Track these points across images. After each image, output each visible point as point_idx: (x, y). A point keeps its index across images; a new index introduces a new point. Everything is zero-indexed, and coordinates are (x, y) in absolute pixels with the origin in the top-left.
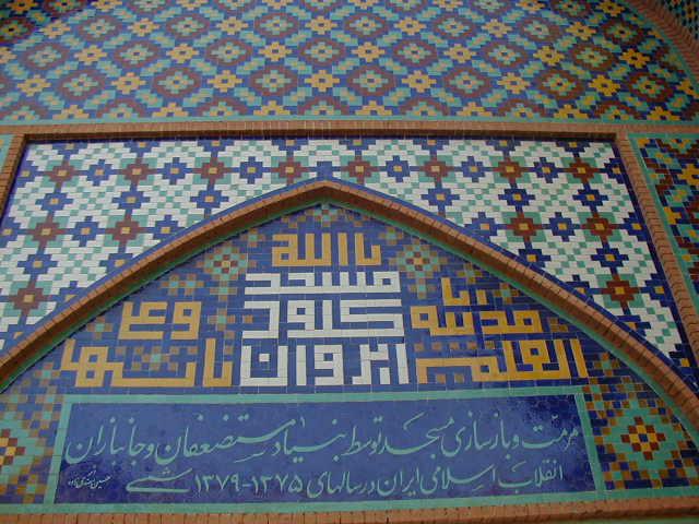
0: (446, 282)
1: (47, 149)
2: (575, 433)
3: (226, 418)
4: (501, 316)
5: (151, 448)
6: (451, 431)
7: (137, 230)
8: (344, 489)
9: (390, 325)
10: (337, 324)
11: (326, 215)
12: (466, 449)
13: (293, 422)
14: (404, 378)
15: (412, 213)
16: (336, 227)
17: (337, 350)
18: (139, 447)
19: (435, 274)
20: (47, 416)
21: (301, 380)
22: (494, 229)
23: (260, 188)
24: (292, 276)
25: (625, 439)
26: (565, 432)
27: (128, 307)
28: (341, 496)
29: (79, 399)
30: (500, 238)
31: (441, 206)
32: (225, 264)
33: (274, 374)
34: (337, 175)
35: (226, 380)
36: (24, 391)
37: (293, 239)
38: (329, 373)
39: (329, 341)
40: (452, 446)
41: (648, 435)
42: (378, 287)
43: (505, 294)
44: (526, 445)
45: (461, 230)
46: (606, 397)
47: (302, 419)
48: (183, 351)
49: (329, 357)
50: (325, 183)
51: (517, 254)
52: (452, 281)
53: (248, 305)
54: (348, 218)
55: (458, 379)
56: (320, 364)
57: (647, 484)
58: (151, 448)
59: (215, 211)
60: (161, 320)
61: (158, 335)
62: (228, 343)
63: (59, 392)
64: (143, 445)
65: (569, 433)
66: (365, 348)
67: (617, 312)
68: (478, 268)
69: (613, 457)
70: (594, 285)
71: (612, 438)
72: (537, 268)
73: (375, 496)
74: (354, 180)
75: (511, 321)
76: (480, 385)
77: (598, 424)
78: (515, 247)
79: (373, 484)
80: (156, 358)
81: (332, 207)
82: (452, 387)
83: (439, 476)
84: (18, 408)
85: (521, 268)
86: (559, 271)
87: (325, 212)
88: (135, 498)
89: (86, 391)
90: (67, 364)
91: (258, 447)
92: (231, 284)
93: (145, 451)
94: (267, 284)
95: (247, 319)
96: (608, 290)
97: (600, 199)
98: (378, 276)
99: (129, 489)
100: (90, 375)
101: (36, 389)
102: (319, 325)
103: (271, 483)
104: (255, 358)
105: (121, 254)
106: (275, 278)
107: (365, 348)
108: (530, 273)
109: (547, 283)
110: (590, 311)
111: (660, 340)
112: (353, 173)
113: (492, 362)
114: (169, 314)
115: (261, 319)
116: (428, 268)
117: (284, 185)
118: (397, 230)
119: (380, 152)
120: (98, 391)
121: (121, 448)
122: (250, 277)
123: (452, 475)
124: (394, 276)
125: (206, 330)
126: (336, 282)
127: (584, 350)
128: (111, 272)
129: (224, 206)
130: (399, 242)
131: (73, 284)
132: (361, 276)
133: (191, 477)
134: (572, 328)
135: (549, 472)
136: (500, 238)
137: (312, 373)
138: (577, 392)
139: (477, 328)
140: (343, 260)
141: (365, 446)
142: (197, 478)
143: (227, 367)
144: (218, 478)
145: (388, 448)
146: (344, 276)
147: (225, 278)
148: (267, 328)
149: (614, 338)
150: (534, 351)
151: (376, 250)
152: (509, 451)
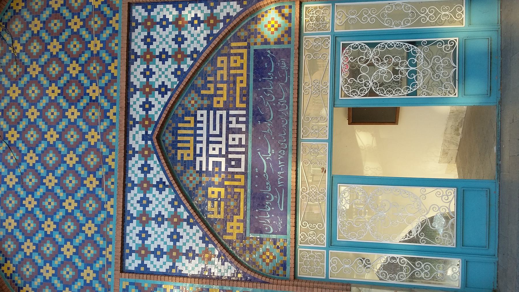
0: (203, 92)
1: (127, 262)
2: (269, 51)
3: (257, 177)
7: (175, 215)
9: (221, 116)
10: (220, 135)
11: (168, 138)
13: (259, 153)
14: (244, 112)
15: (171, 102)
16: (175, 134)
17: (231, 136)
21: (243, 149)
22: (179, 69)
26: (268, 55)
28: (287, 137)
30: (185, 67)
31: (167, 90)
32: (191, 178)
33: (239, 160)
34: (150, 132)
35: (242, 177)
37: (180, 152)
38: (240, 139)
39: (227, 139)
41: (271, 25)
43: (209, 69)
45: (181, 82)
49: (234, 139)
50: (154, 138)
53: (210, 169)
56: (237, 142)
58: (267, 203)
59: (167, 183)
60: (216, 203)
61: (222, 203)
64: (266, 206)
65: (269, 54)
66: (231, 126)
67: (221, 25)
68: (197, 78)
69: (279, 39)
74: (153, 125)
75: (222, 69)
76: (248, 84)
78: (189, 62)
79: (283, 126)
80: (232, 203)
81: (164, 135)
82: (247, 95)
83: (282, 103)
86: (202, 45)
87: (167, 138)
90: (234, 238)
91: (268, 165)
92: (201, 176)
95: (217, 169)
96: (212, 27)
97: (165, 18)
98: (199, 118)
100: (238, 228)
102: (220, 143)
103: (282, 160)
104: (233, 167)
105: (187, 221)
107: (231, 126)
109: (207, 51)
111: (235, 10)
112: (149, 125)
113: (239, 79)
114: (213, 200)
115: (217, 164)
116: (196, 98)
119: (137, 112)
121: (267, 213)
122: (198, 169)
124: (199, 112)
125: (221, 185)
126: (201, 135)
128: (196, 223)
129: (165, 179)
131: (200, 238)
132: (199, 125)
133: (278, 188)
135: (283, 64)
136: (185, 67)
137: (240, 145)
138: (253, 48)
140: (191, 132)
143: (236, 177)
144: (279, 179)
145: (270, 120)
146: (199, 132)
147: (198, 179)
149: (233, 29)
150: (235, 61)
151: (187, 119)
152: (274, 77)
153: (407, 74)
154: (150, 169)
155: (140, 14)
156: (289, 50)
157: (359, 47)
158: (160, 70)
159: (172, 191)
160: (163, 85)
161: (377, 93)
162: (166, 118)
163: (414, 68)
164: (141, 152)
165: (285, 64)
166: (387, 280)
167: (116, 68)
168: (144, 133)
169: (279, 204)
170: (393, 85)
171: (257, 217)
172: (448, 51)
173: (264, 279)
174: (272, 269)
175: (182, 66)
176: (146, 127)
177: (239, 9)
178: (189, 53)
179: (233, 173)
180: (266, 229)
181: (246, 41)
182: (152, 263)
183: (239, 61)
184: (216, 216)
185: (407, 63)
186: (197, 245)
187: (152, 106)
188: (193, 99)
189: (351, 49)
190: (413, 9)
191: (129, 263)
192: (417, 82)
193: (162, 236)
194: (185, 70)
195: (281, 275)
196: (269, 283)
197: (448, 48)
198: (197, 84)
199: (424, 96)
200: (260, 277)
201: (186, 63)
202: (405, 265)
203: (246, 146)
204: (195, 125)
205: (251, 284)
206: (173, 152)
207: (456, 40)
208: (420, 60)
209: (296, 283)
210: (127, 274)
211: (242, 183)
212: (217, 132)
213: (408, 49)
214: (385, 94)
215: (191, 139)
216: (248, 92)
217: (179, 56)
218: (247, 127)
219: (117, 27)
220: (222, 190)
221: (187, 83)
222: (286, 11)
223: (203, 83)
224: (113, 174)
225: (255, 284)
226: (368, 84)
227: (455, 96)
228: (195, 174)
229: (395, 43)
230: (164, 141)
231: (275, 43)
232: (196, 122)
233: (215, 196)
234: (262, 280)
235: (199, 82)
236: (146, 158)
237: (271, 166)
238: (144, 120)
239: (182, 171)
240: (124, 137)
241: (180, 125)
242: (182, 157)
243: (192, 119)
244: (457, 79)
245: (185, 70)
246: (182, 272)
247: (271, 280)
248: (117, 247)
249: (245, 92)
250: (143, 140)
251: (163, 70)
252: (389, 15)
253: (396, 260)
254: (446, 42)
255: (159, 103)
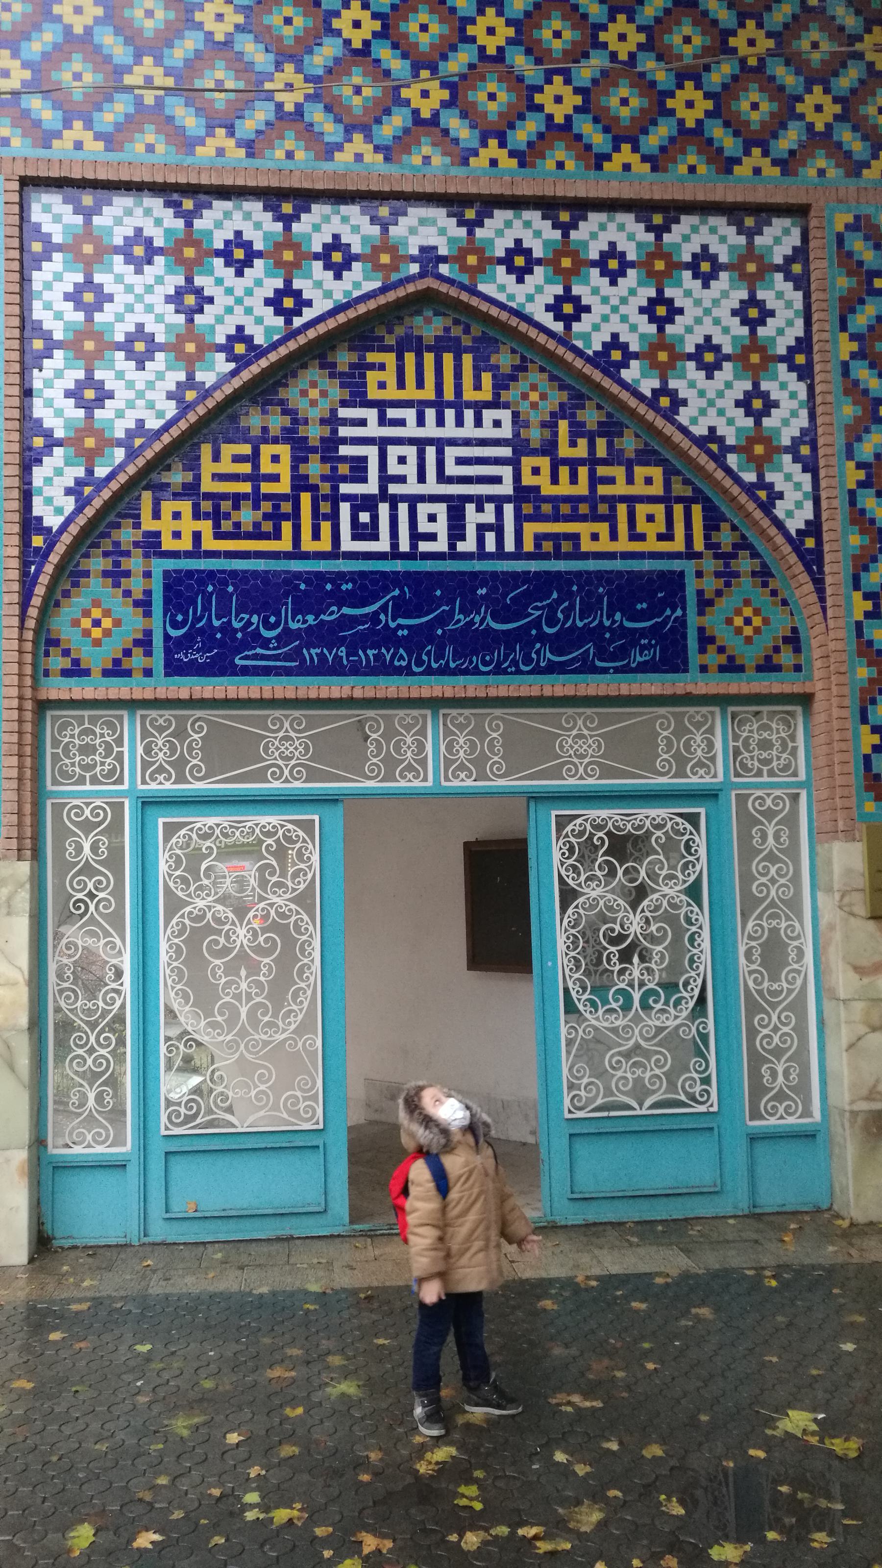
0: (563, 426)
1: (53, 199)
2: (679, 612)
4: (619, 472)
5: (255, 619)
6: (552, 609)
7: (205, 348)
8: (448, 662)
9: (497, 480)
10: (442, 478)
12: (567, 625)
13: (397, 592)
14: (510, 546)
15: (533, 333)
16: (439, 347)
17: (441, 509)
18: (242, 619)
19: (553, 414)
20: (136, 585)
21: (404, 546)
22: (628, 356)
23: (349, 287)
24: (392, 413)
25: (729, 621)
26: (668, 612)
27: (206, 450)
28: (444, 671)
29: (171, 564)
31: (568, 320)
32: (314, 394)
33: (375, 537)
35: (325, 544)
36: (106, 554)
37: (390, 359)
38: (432, 537)
40: (551, 622)
42: (487, 431)
43: (629, 444)
44: (628, 624)
46: (718, 575)
47: (406, 589)
48: (276, 507)
49: (432, 518)
50: (430, 282)
51: (649, 394)
52: (571, 425)
53: (344, 450)
54: (457, 331)
55: (566, 546)
56: (424, 527)
57: (741, 669)
59: (297, 322)
60: (246, 468)
62: (325, 498)
63: (146, 556)
64: (247, 616)
67: (750, 477)
69: (712, 640)
70: (730, 441)
71: (713, 621)
72: (670, 415)
73: (477, 672)
74: (465, 279)
75: (630, 480)
76: (586, 556)
77: (704, 603)
78: (647, 386)
80: (247, 516)
82: (558, 555)
83: (538, 652)
84: (106, 574)
85: (651, 416)
86: (694, 421)
87: (428, 321)
88: (245, 671)
89: (174, 555)
90: (148, 524)
92: (323, 421)
93: (249, 623)
94: (363, 423)
99: (238, 661)
100: (177, 535)
101: (119, 552)
102: (422, 478)
105: (190, 382)
106: (372, 415)
107: (470, 508)
108: (660, 422)
109: (678, 437)
110: (720, 474)
111: (790, 514)
112: (464, 268)
113: (603, 529)
117: (378, 284)
118: (513, 351)
120: (188, 555)
121: (225, 620)
122: (344, 413)
123: (551, 652)
124: (505, 416)
125: (300, 483)
126: (440, 422)
127: (705, 518)
128: (185, 408)
129: (308, 314)
130: (515, 368)
131: (140, 423)
133: (298, 651)
134: (696, 490)
137: (416, 536)
138: (688, 567)
139: (592, 487)
140: (449, 394)
141: (468, 619)
142: (305, 651)
143: (326, 527)
146: (450, 414)
147: (314, 414)
148: (364, 480)
150: (650, 518)
151: (487, 379)
152: (609, 629)
153: (622, 986)
154: (339, 272)
155: (777, 241)
156: (683, 667)
157: (691, 858)
158: (624, 301)
159: (276, 337)
160: (582, 309)
161: (570, 911)
162: (486, 318)
163: (636, 1003)
164: (385, 245)
165: (647, 658)
166: (57, 958)
167: (627, 167)
168: (443, 251)
169: (253, 652)
170: (590, 951)
171: (210, 588)
172: (683, 1087)
173: (33, 612)
174: (63, 637)
175: (634, 363)
176: (458, 258)
177: (794, 525)
178: (672, 384)
179: (334, 517)
180: (180, 618)
181: (708, 546)
182: (58, 277)
183: (651, 530)
184: (208, 467)
185: (651, 986)
186: (120, 414)
187: (521, 275)
188: (543, 397)
189: (686, 837)
190: (790, 991)
191: (51, 205)
192: (600, 1012)
193: (139, 307)
194: (625, 374)
195: (47, 663)
196: (22, 627)
197: (691, 1086)
198: (584, 408)
199: (563, 1030)
200: (36, 601)
201: (644, 375)
202: (101, 1004)
203: (412, 555)
204: (469, 405)
205: (15, 575)
206: (390, 340)
207: (712, 1106)
208: (658, 1019)
209: (29, 705)
210: (16, 198)
211: (308, 544)
212: (451, 469)
213: (686, 984)
214: (566, 931)
215: (428, 393)
216: (568, 556)
217: (663, 356)
218: (466, 556)
219: (743, 171)
220: (284, 487)
221: (587, 379)
222: (786, 657)
223: (588, 428)
224: (317, 158)
225: (16, 587)
226: (594, 884)
227: (566, 1111)
228: (327, 406)
229: (701, 952)
230: (419, 313)
231: (701, 630)
232: (479, 407)
233: (266, 467)
234: (30, 609)
235: (590, 417)
236: (371, 258)
237: (361, 627)
238: (479, 251)
239: (334, 365)
240: (429, 189)
241: (467, 360)
242: (372, 367)
243: (486, 394)
244: (613, 1114)
245: (626, 374)
246: (36, 372)
247: (29, 635)
248: (98, 167)
249: (566, 547)
250: (423, 249)
251: (623, 309)
252: (774, 931)
253: (114, 981)
254: (706, 1081)
255: (530, 298)
